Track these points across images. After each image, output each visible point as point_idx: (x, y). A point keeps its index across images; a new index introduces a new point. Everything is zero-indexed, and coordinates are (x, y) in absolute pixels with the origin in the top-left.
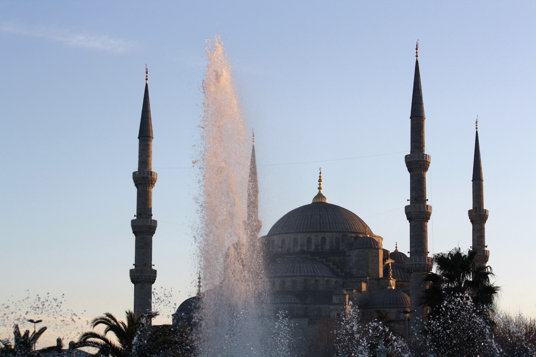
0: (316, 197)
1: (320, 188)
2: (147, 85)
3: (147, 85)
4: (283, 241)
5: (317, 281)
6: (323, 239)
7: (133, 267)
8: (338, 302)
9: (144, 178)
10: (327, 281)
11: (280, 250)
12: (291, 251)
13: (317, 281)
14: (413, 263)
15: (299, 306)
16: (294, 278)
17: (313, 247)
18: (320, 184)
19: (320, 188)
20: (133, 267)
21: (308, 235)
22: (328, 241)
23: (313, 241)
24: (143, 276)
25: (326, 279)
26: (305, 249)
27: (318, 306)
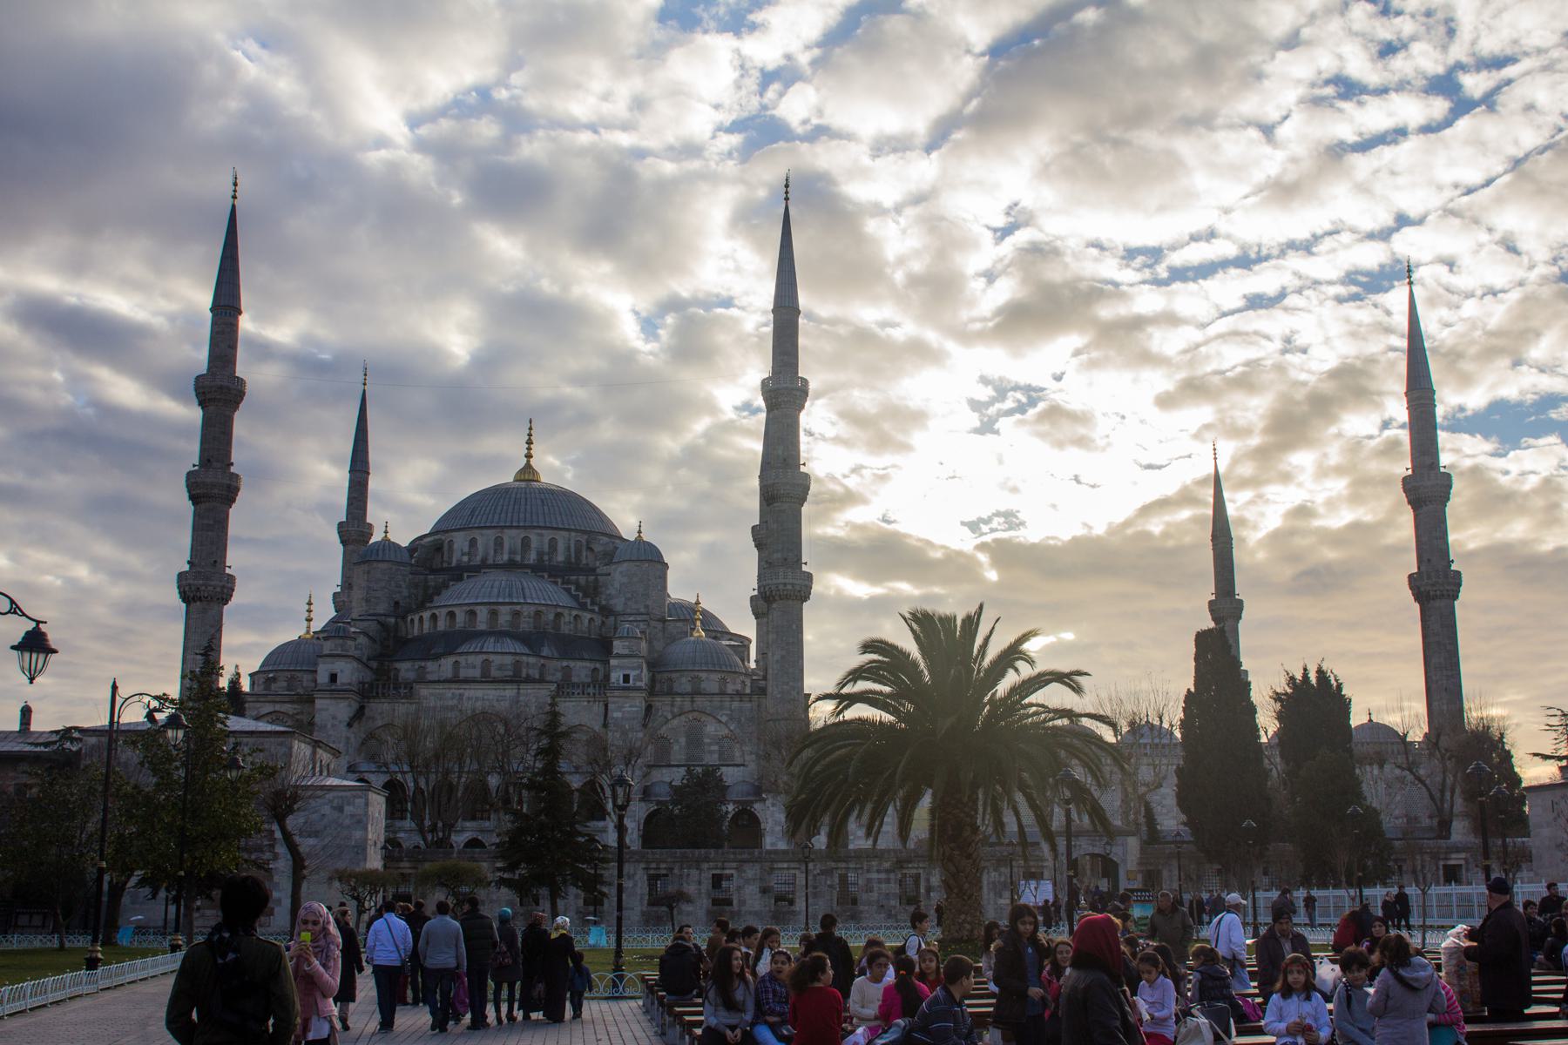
0: (522, 471)
1: (529, 456)
2: (234, 206)
3: (234, 206)
4: (473, 542)
5: (558, 615)
6: (553, 544)
7: (187, 567)
8: (626, 652)
9: (221, 387)
10: (576, 617)
11: (465, 559)
12: (490, 561)
13: (558, 615)
14: (781, 580)
15: (532, 660)
16: (518, 608)
17: (532, 557)
18: (529, 449)
19: (529, 456)
20: (187, 567)
21: (523, 534)
22: (561, 546)
23: (534, 544)
24: (205, 590)
25: (574, 613)
26: (518, 558)
27: (565, 663)
